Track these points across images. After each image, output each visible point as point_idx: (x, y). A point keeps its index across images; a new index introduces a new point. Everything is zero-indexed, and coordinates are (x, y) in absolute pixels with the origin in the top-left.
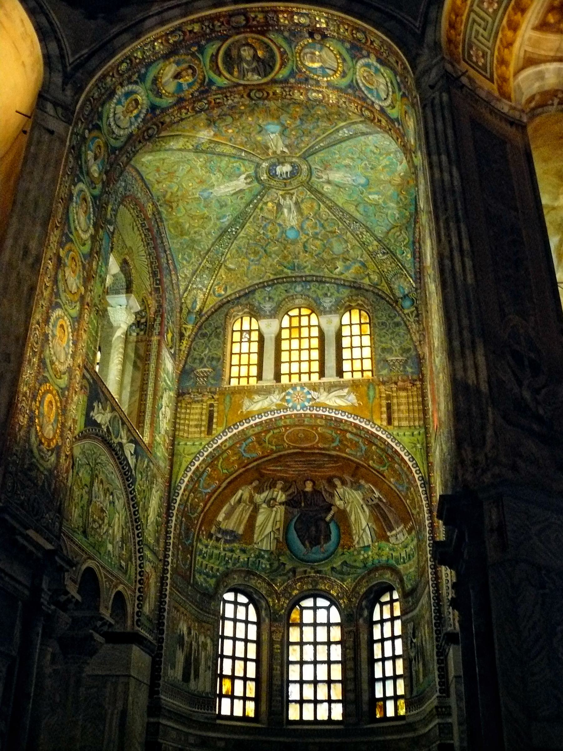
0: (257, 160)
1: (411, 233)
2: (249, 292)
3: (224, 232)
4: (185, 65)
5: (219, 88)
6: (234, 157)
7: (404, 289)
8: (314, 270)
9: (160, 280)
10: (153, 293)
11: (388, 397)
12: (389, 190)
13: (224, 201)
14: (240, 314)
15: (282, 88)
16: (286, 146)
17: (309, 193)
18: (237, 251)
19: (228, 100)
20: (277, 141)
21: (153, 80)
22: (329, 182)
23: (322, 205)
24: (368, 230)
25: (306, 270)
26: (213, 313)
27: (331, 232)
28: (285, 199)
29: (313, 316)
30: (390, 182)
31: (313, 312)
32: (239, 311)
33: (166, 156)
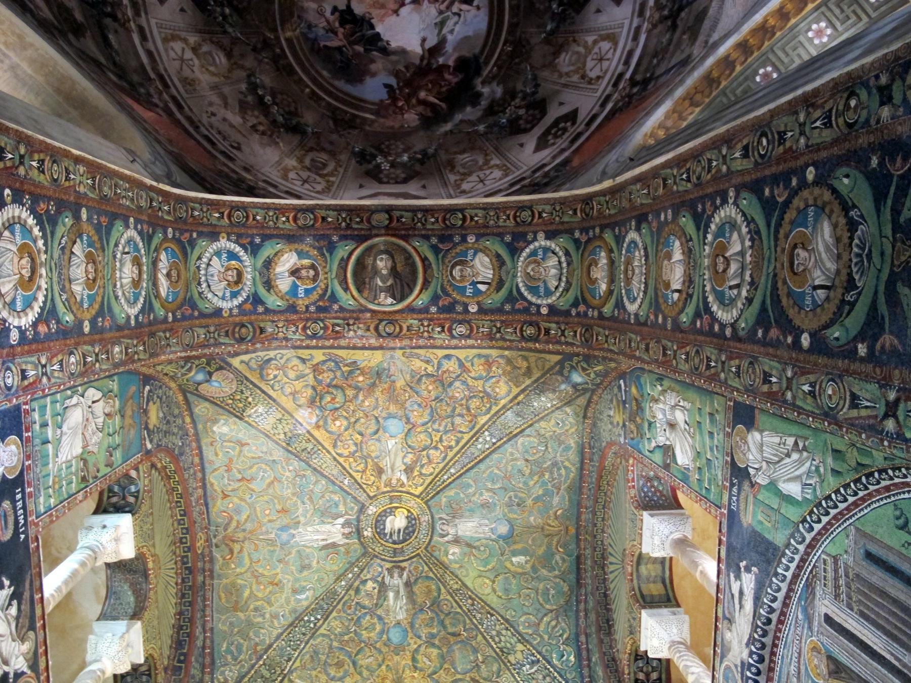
0: (363, 498)
1: (573, 620)
3: (298, 620)
4: (306, 262)
5: (342, 309)
6: (333, 483)
9: (185, 655)
10: (169, 672)
12: (540, 546)
13: (308, 557)
15: (420, 320)
16: (405, 470)
17: (426, 568)
18: (312, 656)
19: (349, 330)
20: (396, 455)
21: (265, 261)
22: (457, 541)
24: (510, 624)
27: (454, 634)
28: (392, 577)
30: (543, 528)
33: (246, 439)
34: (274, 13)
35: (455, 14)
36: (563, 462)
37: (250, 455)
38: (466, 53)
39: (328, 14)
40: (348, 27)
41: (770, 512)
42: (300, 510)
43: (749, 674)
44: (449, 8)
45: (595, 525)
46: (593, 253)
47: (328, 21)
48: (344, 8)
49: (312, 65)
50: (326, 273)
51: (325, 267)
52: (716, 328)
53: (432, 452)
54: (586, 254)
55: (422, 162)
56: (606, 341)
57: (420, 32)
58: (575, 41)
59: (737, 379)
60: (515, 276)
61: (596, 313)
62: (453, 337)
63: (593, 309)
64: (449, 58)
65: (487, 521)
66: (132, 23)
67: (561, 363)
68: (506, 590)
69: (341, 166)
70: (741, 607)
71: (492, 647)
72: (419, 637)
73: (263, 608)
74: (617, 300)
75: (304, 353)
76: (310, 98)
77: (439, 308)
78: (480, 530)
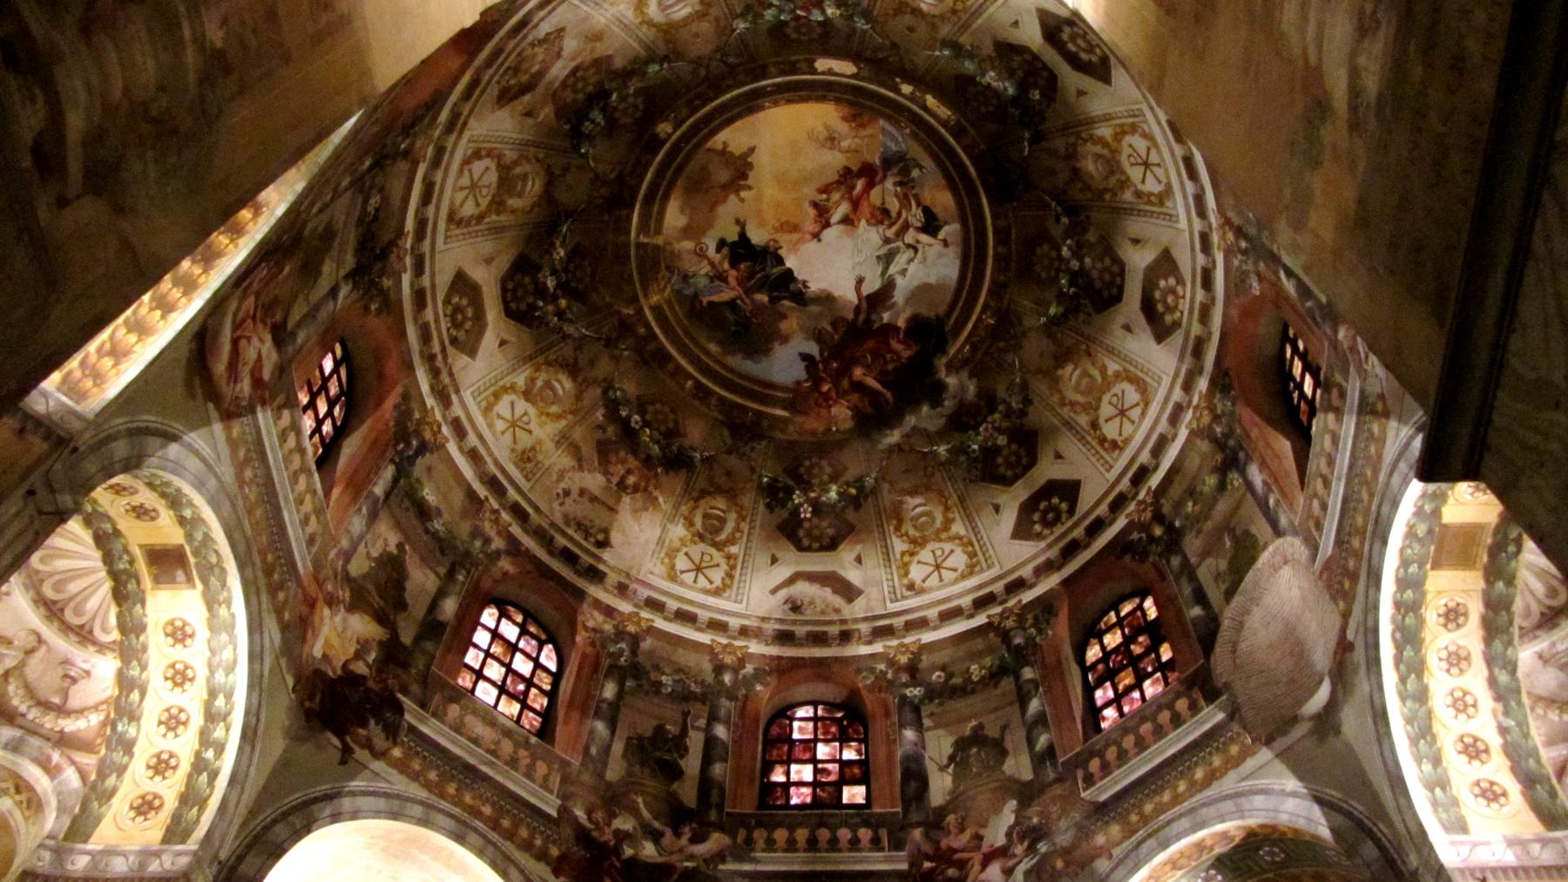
34: (631, 275)
35: (909, 246)
38: (925, 311)
39: (712, 252)
40: (742, 266)
44: (900, 234)
47: (712, 264)
48: (736, 238)
49: (693, 339)
55: (856, 502)
57: (853, 268)
58: (1090, 355)
64: (898, 315)
66: (445, 430)
69: (744, 519)
76: (695, 396)
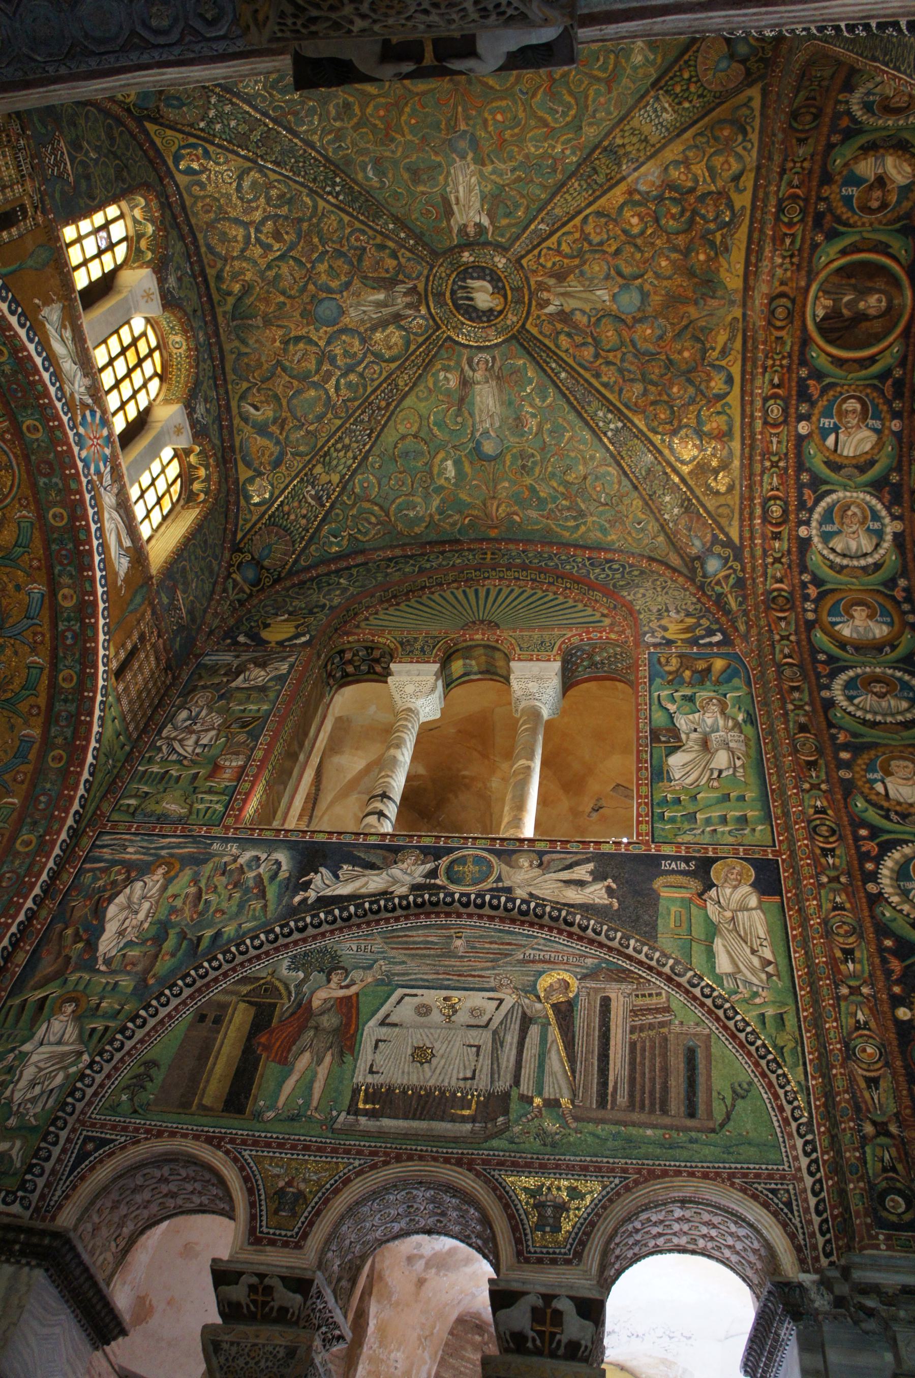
2: (178, 226)
5: (815, 246)
7: (268, 556)
8: (237, 359)
11: (142, 637)
12: (470, 495)
14: (137, 213)
15: (790, 356)
16: (562, 312)
17: (421, 340)
19: (784, 258)
20: (586, 300)
22: (465, 383)
23: (393, 366)
25: (237, 343)
26: (141, 146)
28: (405, 294)
29: (156, 382)
31: (162, 378)
32: (147, 209)
36: (585, 523)
37: (591, 93)
41: (685, 925)
42: (502, 166)
43: (503, 899)
45: (509, 569)
46: (885, 612)
50: (871, 224)
51: (880, 223)
52: (870, 866)
53: (592, 350)
54: (881, 600)
56: (783, 638)
59: (830, 906)
60: (845, 487)
61: (810, 616)
62: (765, 400)
63: (815, 611)
65: (497, 425)
67: (729, 543)
68: (407, 453)
70: (568, 882)
71: (328, 441)
72: (328, 343)
73: (350, 119)
74: (838, 659)
75: (748, 181)
77: (805, 379)
78: (484, 417)
